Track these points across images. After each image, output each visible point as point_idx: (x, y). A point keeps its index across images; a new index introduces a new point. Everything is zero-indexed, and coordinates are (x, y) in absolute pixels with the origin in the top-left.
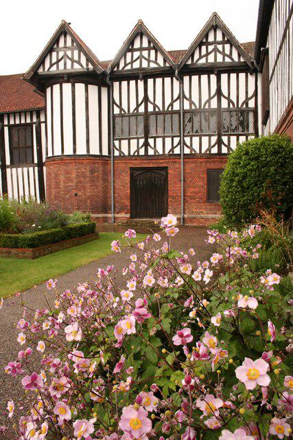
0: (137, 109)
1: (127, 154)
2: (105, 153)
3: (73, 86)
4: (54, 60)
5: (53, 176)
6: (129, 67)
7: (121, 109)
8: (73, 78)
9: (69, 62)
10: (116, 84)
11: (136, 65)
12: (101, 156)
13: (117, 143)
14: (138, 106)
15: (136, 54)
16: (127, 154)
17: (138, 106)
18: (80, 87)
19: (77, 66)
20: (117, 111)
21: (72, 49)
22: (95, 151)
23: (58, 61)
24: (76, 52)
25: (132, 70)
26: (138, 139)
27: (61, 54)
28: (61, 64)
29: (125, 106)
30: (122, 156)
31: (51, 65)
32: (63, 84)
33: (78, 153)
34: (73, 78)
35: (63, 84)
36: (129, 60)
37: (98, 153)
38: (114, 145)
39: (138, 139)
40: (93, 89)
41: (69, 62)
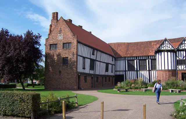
0: (183, 58)
1: (181, 69)
2: (175, 69)
3: (167, 53)
4: (163, 47)
5: (161, 74)
6: (181, 48)
7: (179, 58)
8: (168, 51)
9: (167, 47)
10: (177, 52)
11: (183, 48)
12: (174, 70)
13: (178, 66)
14: (184, 57)
15: (183, 45)
16: (181, 69)
17: (184, 57)
18: (169, 53)
19: (169, 48)
20: (178, 59)
21: (168, 44)
22: (173, 69)
23: (164, 47)
24: (169, 45)
25: (182, 49)
26: (184, 66)
27: (165, 45)
28: (165, 48)
29: (180, 58)
30: (179, 70)
31: (162, 48)
32: (165, 52)
33: (169, 69)
34: (168, 51)
35: (165, 52)
36: (181, 47)
37: (173, 69)
38: (177, 67)
39: (184, 66)
40: (172, 53)
41: (167, 47)
